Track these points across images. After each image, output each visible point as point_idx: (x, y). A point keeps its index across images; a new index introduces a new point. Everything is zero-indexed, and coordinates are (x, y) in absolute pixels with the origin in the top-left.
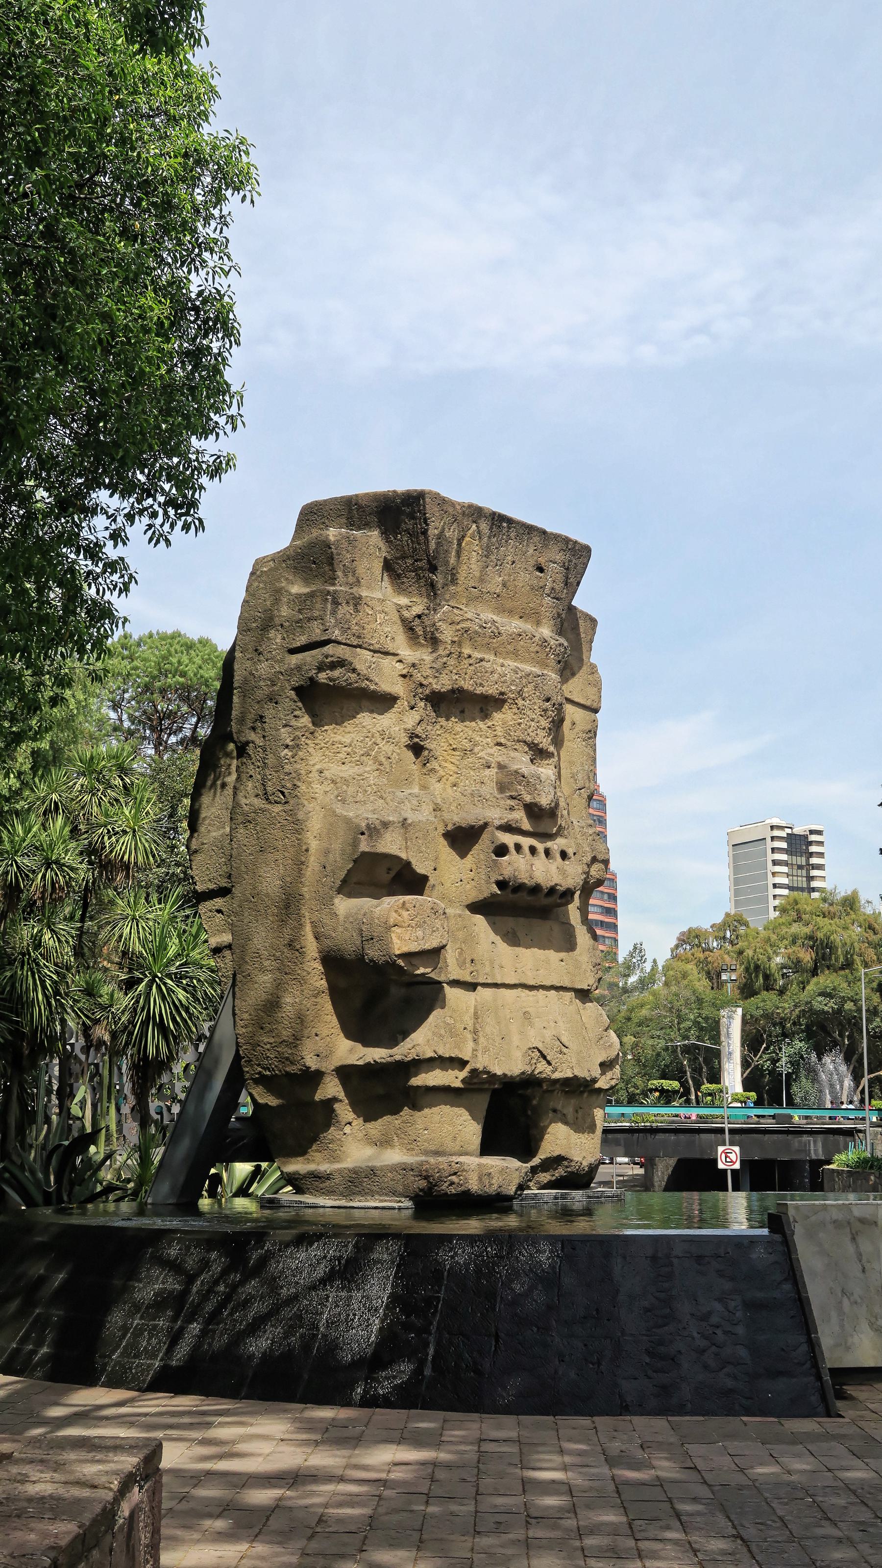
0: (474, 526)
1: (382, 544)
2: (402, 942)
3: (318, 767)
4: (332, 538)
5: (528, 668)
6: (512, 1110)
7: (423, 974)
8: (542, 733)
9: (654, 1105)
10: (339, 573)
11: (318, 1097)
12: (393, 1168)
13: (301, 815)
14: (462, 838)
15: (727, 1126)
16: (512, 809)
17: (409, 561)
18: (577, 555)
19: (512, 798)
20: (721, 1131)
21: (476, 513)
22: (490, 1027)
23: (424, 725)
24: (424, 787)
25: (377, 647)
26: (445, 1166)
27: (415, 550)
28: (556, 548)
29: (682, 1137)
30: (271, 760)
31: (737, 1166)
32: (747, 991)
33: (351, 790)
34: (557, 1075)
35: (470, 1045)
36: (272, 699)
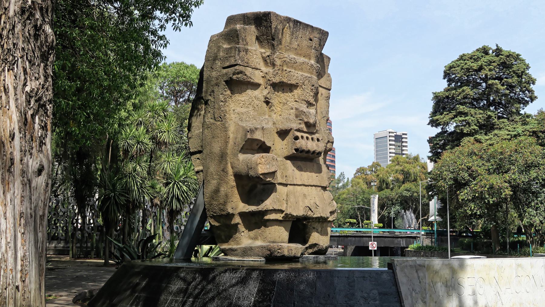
1: (255, 31)
2: (262, 170)
3: (233, 108)
4: (238, 28)
5: (306, 74)
6: (299, 228)
8: (311, 97)
9: (347, 228)
10: (241, 41)
11: (233, 223)
12: (258, 247)
13: (227, 125)
14: (283, 134)
15: (372, 235)
16: (300, 124)
17: (265, 37)
18: (324, 35)
19: (300, 120)
20: (371, 237)
21: (288, 20)
22: (292, 199)
23: (270, 94)
24: (270, 116)
25: (254, 67)
26: (276, 247)
27: (267, 33)
28: (316, 33)
29: (357, 238)
30: (216, 106)
31: (376, 249)
32: (380, 189)
33: (244, 117)
34: (315, 216)
35: (285, 205)
36: (217, 85)
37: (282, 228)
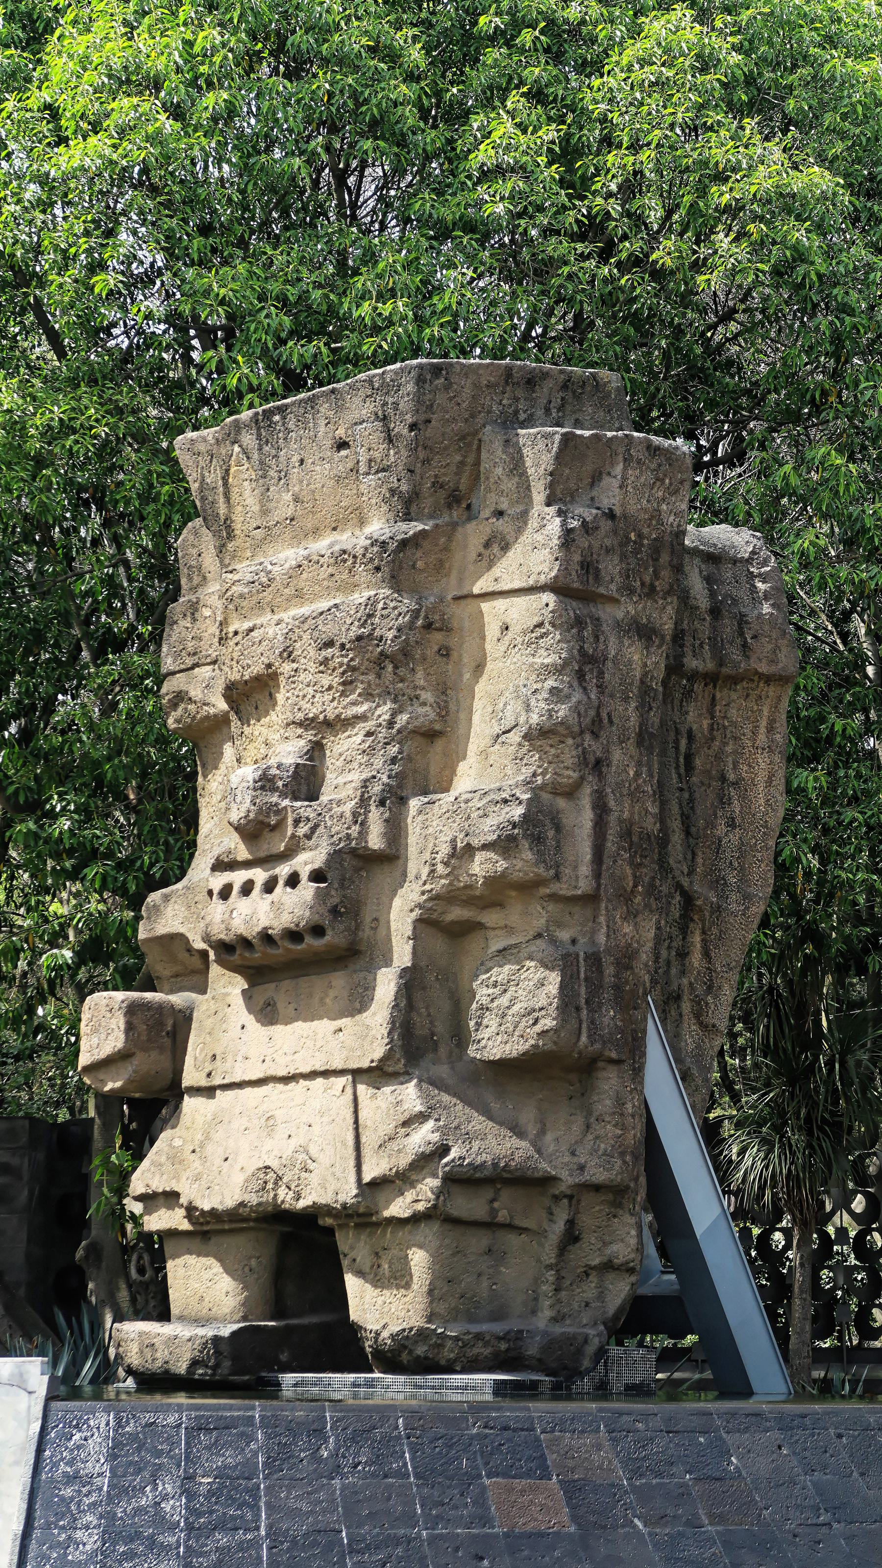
0: (237, 448)
7: (111, 1090)
28: (357, 401)
37: (211, 1261)
